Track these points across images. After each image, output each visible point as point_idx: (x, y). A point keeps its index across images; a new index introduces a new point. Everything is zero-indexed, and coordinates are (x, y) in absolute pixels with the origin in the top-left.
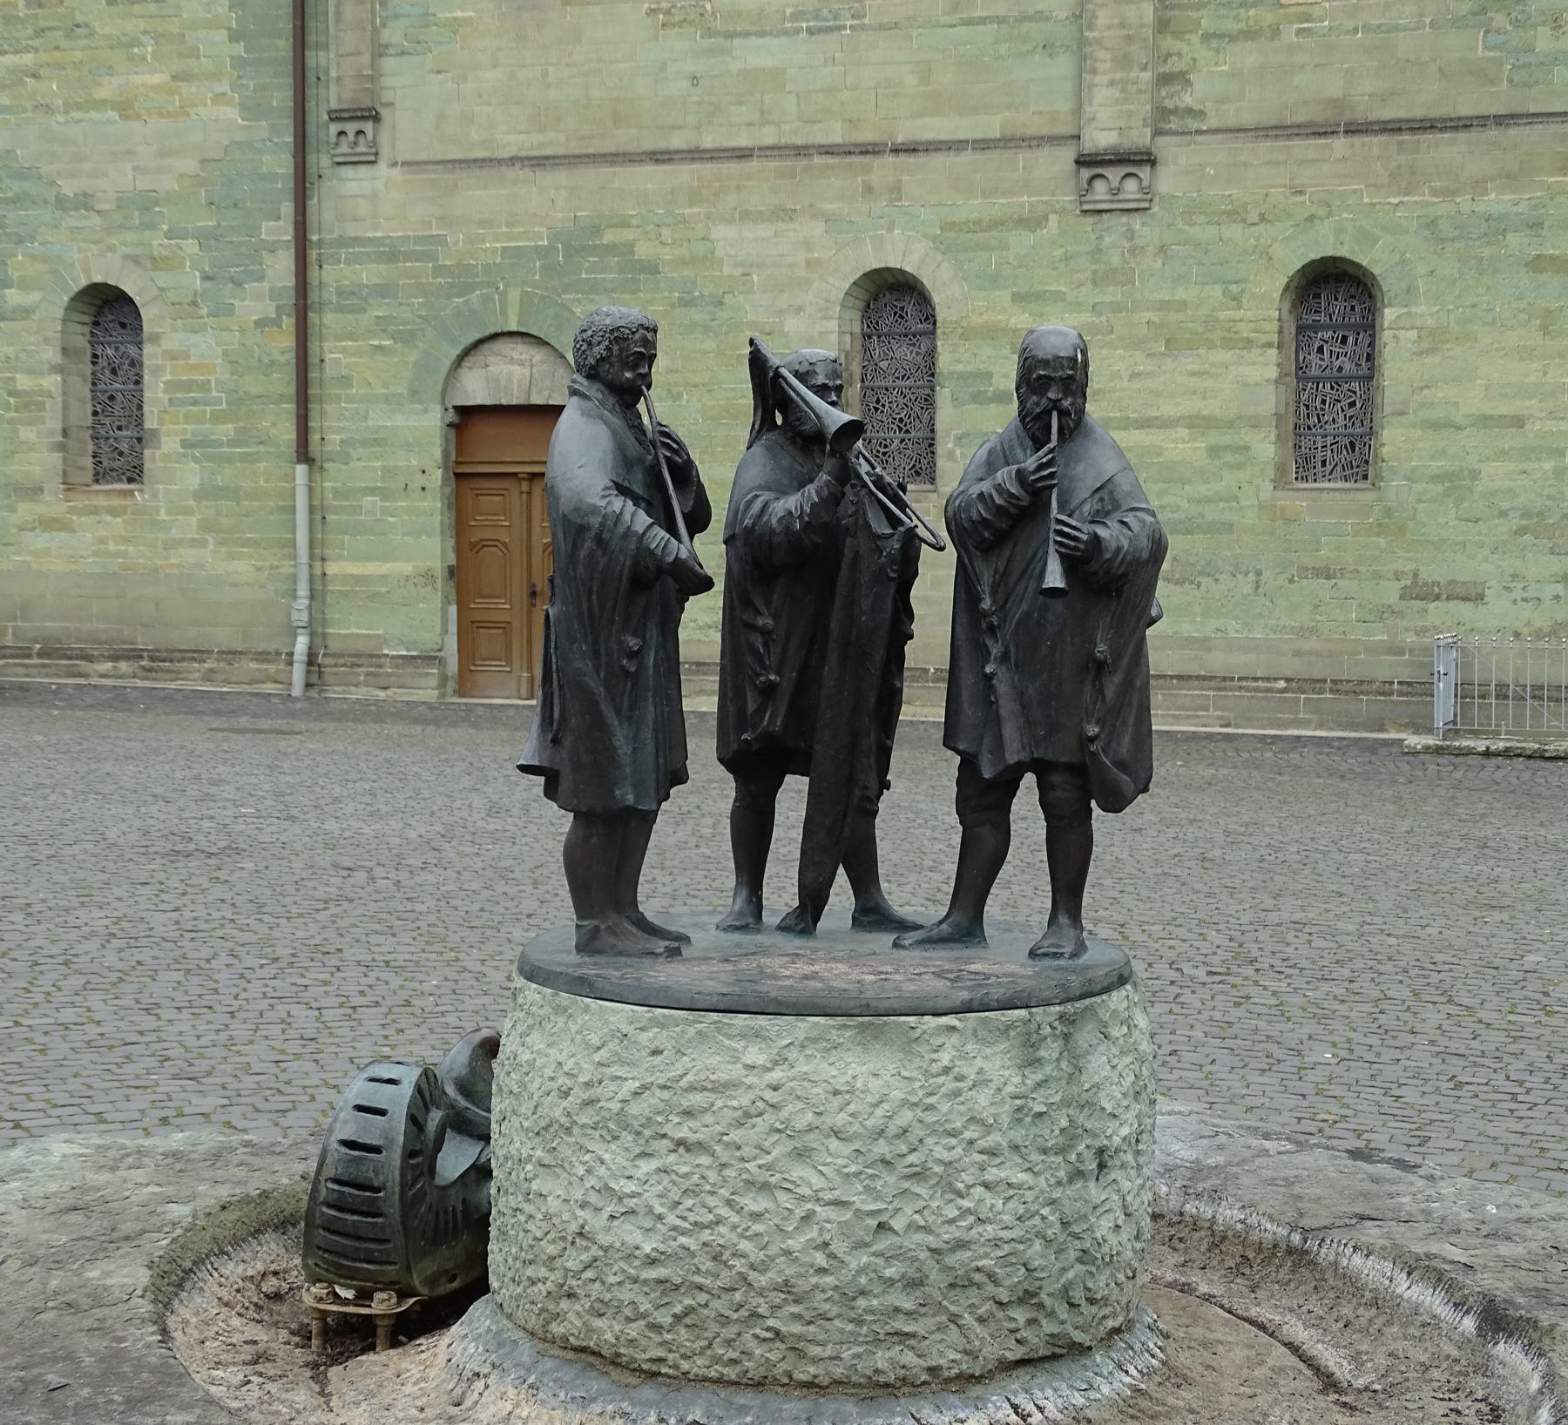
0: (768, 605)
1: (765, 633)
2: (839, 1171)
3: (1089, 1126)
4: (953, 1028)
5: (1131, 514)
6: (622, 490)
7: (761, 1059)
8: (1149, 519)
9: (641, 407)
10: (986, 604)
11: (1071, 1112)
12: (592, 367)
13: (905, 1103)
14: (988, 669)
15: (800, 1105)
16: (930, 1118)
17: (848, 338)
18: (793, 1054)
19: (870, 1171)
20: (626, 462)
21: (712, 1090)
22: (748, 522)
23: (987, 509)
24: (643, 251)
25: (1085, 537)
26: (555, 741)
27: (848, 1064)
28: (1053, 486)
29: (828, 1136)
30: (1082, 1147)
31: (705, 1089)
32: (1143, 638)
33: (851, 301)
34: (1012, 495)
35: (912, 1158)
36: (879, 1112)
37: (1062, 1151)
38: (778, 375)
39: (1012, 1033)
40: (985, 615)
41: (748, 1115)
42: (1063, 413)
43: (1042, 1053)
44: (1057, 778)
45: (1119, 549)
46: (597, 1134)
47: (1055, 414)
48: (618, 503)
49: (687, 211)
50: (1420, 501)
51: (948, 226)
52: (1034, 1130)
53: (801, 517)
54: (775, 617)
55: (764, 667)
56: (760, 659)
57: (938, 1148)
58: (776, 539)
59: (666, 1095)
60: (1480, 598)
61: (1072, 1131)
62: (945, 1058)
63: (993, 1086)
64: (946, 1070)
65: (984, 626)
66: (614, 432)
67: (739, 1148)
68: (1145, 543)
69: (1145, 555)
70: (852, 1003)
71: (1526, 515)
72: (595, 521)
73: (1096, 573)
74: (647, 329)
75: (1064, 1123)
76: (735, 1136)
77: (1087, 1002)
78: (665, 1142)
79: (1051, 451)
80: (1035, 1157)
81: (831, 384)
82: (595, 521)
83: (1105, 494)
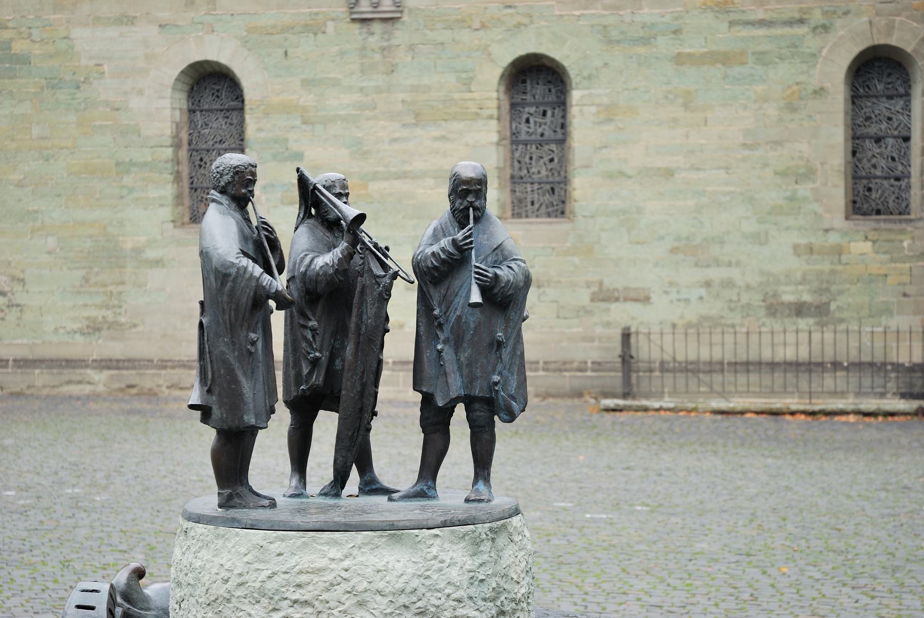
0: (314, 315)
1: (313, 330)
2: (381, 612)
3: (506, 587)
4: (437, 536)
5: (513, 262)
6: (246, 254)
7: (339, 555)
8: (523, 265)
9: (250, 207)
10: (436, 312)
11: (497, 579)
12: (223, 187)
13: (414, 575)
14: (439, 347)
15: (360, 578)
16: (427, 582)
17: (177, 113)
18: (355, 552)
19: (398, 612)
20: (244, 238)
21: (312, 573)
22: (302, 269)
23: (437, 260)
24: (19, 47)
25: (490, 275)
26: (209, 391)
27: (384, 556)
28: (472, 248)
29: (375, 594)
30: (503, 598)
31: (308, 572)
32: (520, 328)
33: (180, 86)
35: (419, 604)
36: (401, 580)
37: (493, 600)
38: (315, 188)
39: (467, 538)
40: (436, 318)
41: (332, 585)
42: (475, 209)
43: (482, 548)
44: (477, 406)
45: (509, 281)
46: (246, 601)
47: (471, 209)
48: (245, 262)
49: (52, 17)
50: (602, 230)
51: (251, 30)
52: (479, 589)
53: (333, 266)
54: (318, 322)
55: (313, 349)
56: (310, 345)
57: (432, 598)
58: (320, 278)
59: (286, 576)
60: (646, 300)
61: (497, 589)
62: (434, 551)
63: (459, 565)
64: (435, 557)
65: (436, 324)
66: (237, 223)
67: (327, 602)
68: (521, 277)
69: (521, 284)
70: (385, 524)
71: (678, 239)
72: (233, 271)
73: (497, 294)
74: (253, 166)
75: (494, 585)
76: (325, 596)
77: (502, 522)
78: (286, 602)
79: (470, 229)
80: (481, 603)
82: (233, 271)
83: (498, 251)
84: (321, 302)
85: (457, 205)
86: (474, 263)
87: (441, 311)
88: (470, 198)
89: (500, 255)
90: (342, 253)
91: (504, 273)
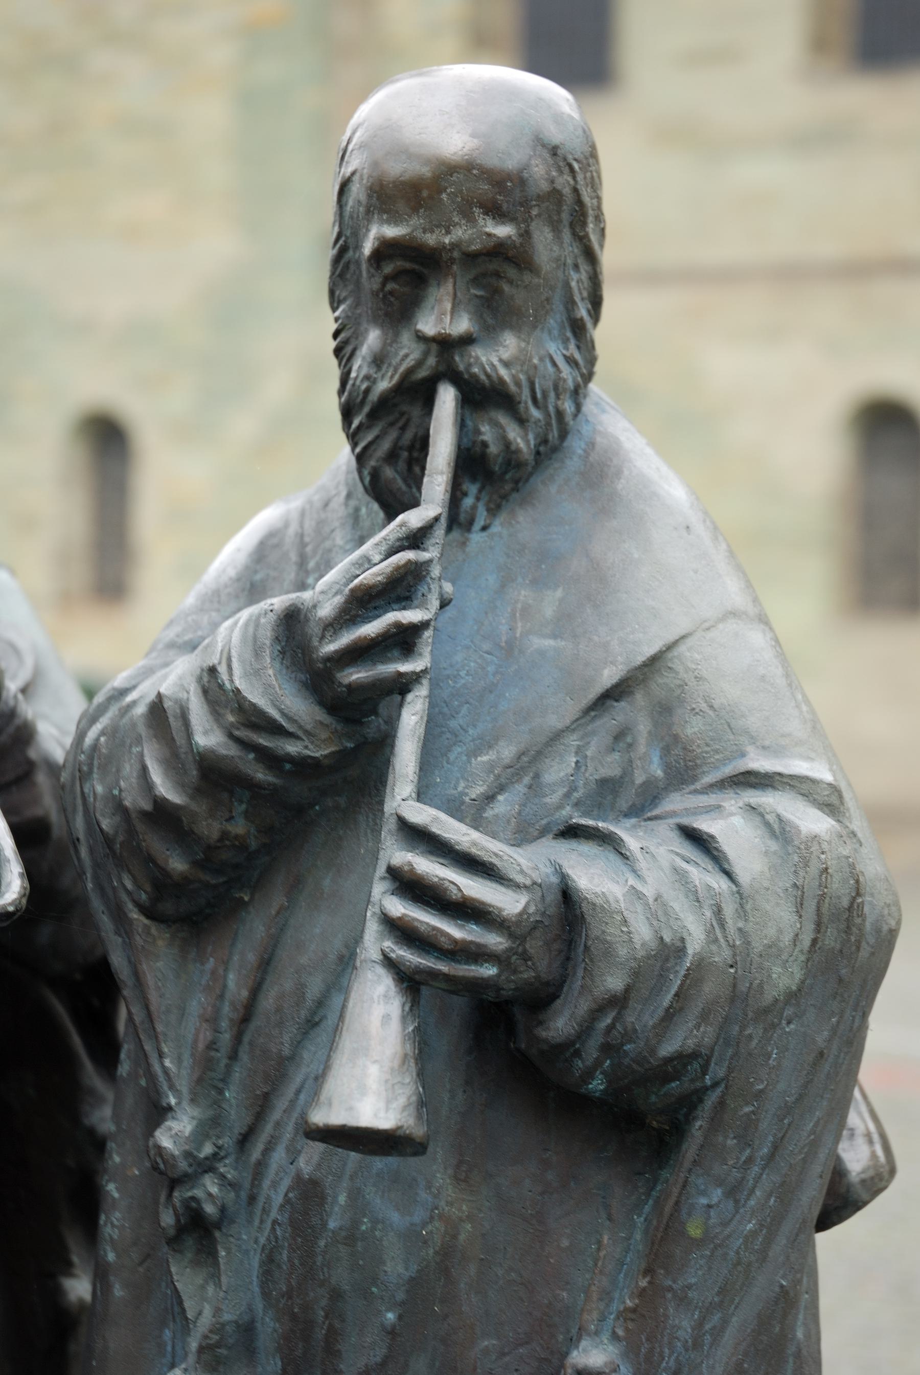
5: (732, 802)
8: (811, 822)
25: (508, 902)
28: (402, 686)
34: (255, 719)
42: (480, 396)
47: (447, 398)
69: (784, 977)
73: (567, 1049)
79: (416, 539)
83: (635, 713)
85: (359, 367)
86: (402, 798)
87: (209, 1127)
88: (442, 315)
89: (648, 741)
91: (638, 888)
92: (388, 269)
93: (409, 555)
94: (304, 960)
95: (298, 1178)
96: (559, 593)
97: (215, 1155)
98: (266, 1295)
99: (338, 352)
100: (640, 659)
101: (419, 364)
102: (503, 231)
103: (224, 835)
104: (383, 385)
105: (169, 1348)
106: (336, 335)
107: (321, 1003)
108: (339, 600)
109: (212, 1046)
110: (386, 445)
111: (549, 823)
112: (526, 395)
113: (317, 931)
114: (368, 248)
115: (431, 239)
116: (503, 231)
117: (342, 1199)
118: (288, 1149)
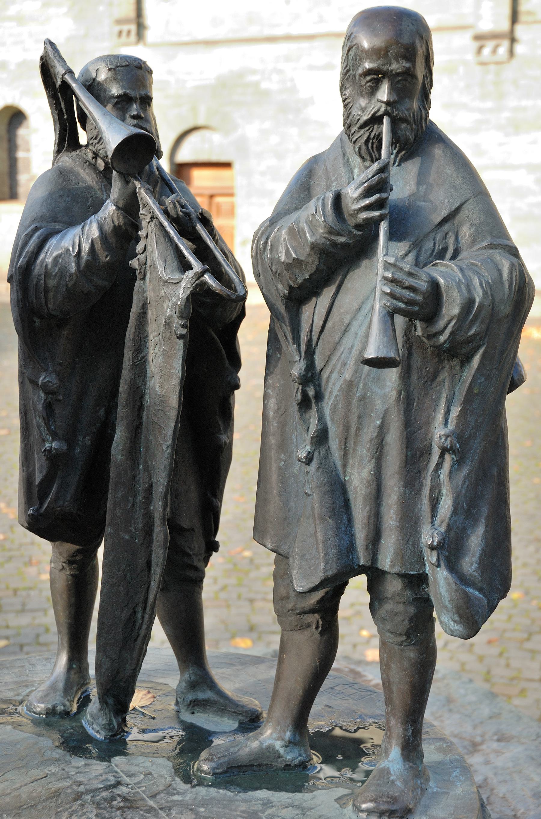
28: (382, 218)
53: (79, 255)
54: (60, 376)
58: (52, 283)
81: (132, 93)
84: (65, 332)
90: (101, 228)
92: (368, 78)
93: (383, 176)
94: (342, 311)
95: (345, 380)
96: (425, 187)
97: (312, 376)
98: (333, 420)
99: (345, 106)
100: (453, 208)
101: (378, 110)
102: (408, 65)
103: (317, 270)
104: (365, 118)
105: (295, 441)
106: (344, 101)
107: (349, 324)
108: (360, 191)
109: (310, 341)
110: (365, 138)
111: (426, 263)
112: (412, 121)
113: (347, 301)
114: (360, 71)
115: (384, 68)
116: (408, 65)
117: (361, 386)
118: (338, 372)
